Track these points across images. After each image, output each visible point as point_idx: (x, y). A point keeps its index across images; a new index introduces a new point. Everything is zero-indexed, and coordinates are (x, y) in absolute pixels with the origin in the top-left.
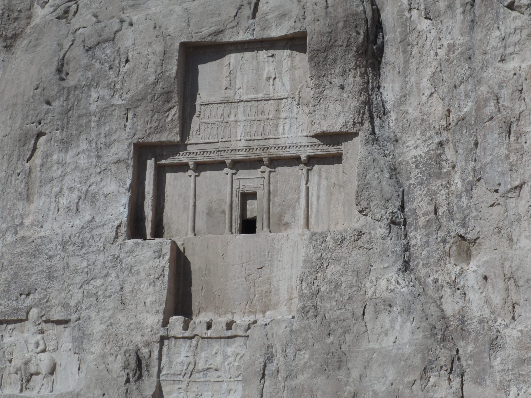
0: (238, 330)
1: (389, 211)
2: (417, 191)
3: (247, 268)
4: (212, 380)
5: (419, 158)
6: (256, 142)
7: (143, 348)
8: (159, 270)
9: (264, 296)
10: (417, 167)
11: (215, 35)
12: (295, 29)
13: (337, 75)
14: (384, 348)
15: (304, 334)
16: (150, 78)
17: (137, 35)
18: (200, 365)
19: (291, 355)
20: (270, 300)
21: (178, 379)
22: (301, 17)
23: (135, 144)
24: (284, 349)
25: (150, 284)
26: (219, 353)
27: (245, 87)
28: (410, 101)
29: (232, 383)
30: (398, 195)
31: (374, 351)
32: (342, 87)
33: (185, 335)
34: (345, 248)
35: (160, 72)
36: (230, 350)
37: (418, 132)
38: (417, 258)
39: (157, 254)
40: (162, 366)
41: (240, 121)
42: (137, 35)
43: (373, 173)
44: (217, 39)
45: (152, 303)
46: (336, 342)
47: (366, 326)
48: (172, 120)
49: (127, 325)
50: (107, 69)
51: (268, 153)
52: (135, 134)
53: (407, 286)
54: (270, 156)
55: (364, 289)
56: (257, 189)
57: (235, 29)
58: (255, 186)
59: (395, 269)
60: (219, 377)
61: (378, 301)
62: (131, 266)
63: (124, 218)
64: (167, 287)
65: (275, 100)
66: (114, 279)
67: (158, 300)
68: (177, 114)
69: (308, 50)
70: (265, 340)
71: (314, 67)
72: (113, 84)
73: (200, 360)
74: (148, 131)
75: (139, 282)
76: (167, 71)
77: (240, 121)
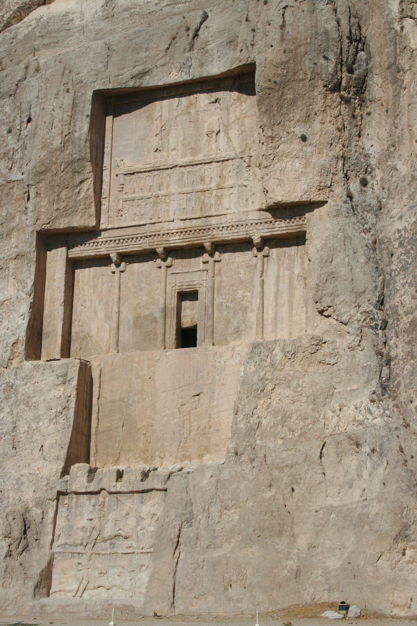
0: (156, 482)
1: (362, 309)
2: (400, 280)
3: (180, 395)
4: (120, 552)
5: (403, 232)
7: (34, 509)
8: (63, 401)
10: (401, 245)
11: (140, 78)
12: (240, 61)
13: (298, 121)
14: (346, 505)
15: (234, 486)
16: (54, 142)
17: (42, 85)
18: (106, 531)
19: (215, 516)
21: (79, 551)
22: (249, 44)
23: (37, 232)
24: (207, 507)
25: (50, 421)
26: (131, 514)
27: (180, 147)
28: (399, 153)
29: (145, 555)
30: (376, 287)
31: (331, 509)
32: (304, 138)
33: (89, 490)
34: (298, 364)
35: (66, 133)
36: (146, 509)
37: (405, 196)
38: (397, 375)
39: (61, 379)
40: (57, 532)
41: (173, 194)
42: (42, 85)
43: (342, 257)
44: (142, 83)
45: (52, 446)
46: (280, 497)
47: (324, 474)
48: (85, 198)
49: (17, 477)
50: (5, 132)
51: (209, 237)
52: (38, 219)
53: (381, 416)
55: (323, 421)
56: (198, 286)
57: (165, 68)
59: (367, 392)
60: (129, 547)
61: (342, 437)
62: (29, 397)
63: (22, 334)
64: (72, 424)
65: (218, 162)
66: (6, 415)
67: (59, 442)
68: (92, 189)
69: (257, 90)
70: (184, 495)
71: (265, 112)
72: (11, 153)
73: (106, 524)
74: (55, 214)
75: (37, 418)
76: (76, 131)
77: (173, 194)
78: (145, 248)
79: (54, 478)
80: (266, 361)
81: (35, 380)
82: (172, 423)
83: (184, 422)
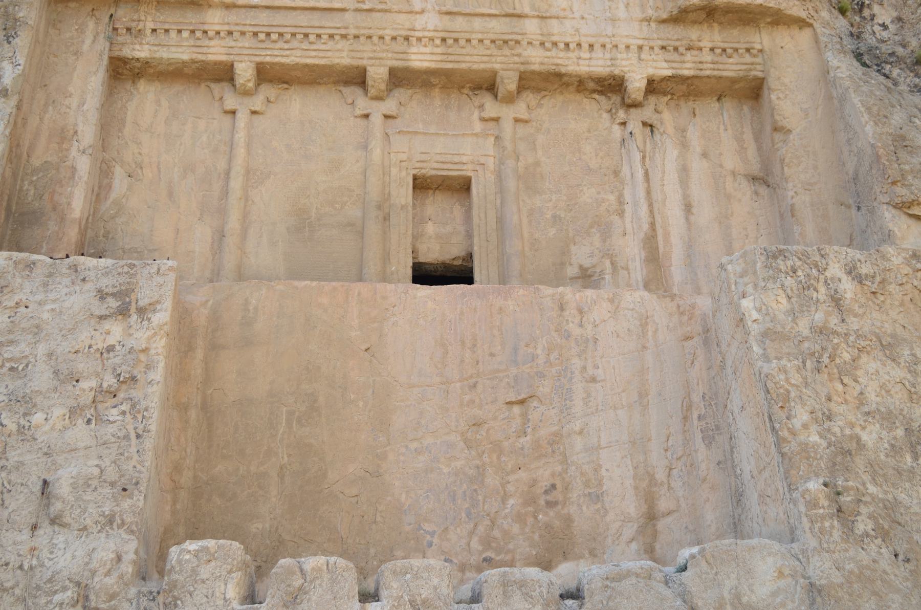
3: (467, 398)
6: (477, 23)
9: (543, 503)
20: (568, 520)
25: (74, 412)
39: (113, 303)
51: (516, 59)
54: (522, 68)
56: (470, 167)
58: (464, 159)
64: (153, 428)
78: (337, 61)
79: (109, 581)
80: (816, 290)
81: (16, 298)
82: (446, 470)
83: (481, 470)
